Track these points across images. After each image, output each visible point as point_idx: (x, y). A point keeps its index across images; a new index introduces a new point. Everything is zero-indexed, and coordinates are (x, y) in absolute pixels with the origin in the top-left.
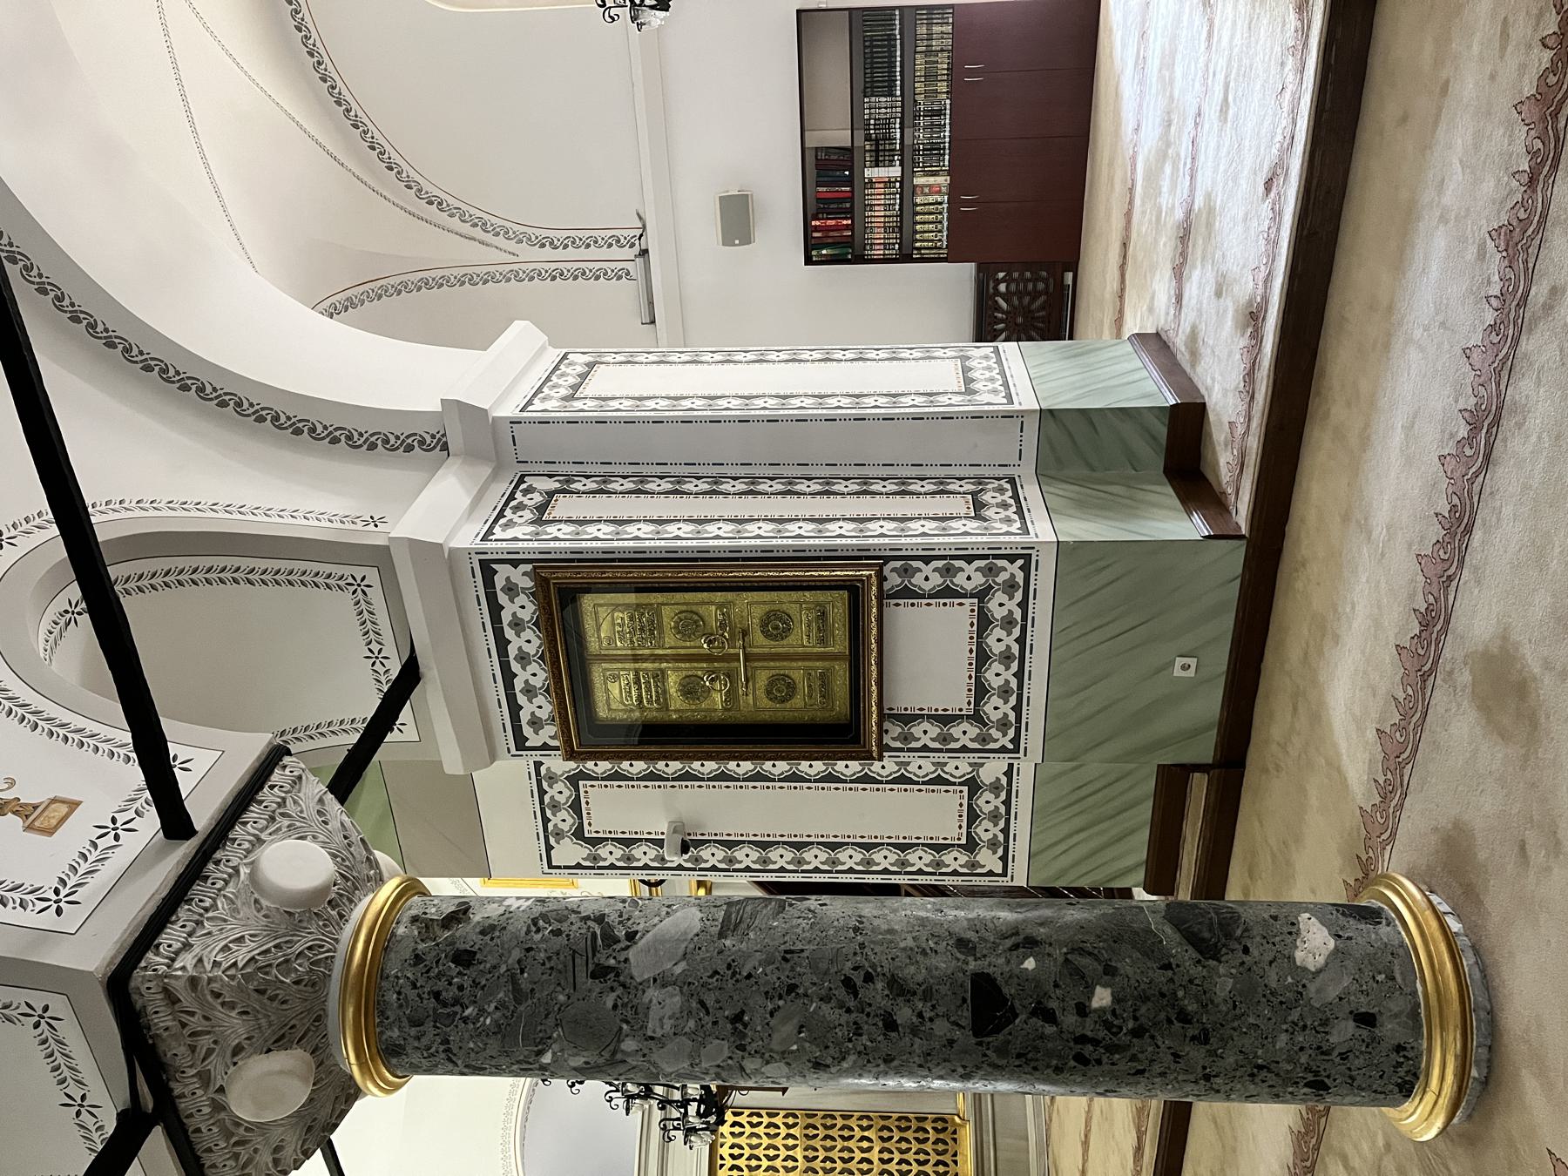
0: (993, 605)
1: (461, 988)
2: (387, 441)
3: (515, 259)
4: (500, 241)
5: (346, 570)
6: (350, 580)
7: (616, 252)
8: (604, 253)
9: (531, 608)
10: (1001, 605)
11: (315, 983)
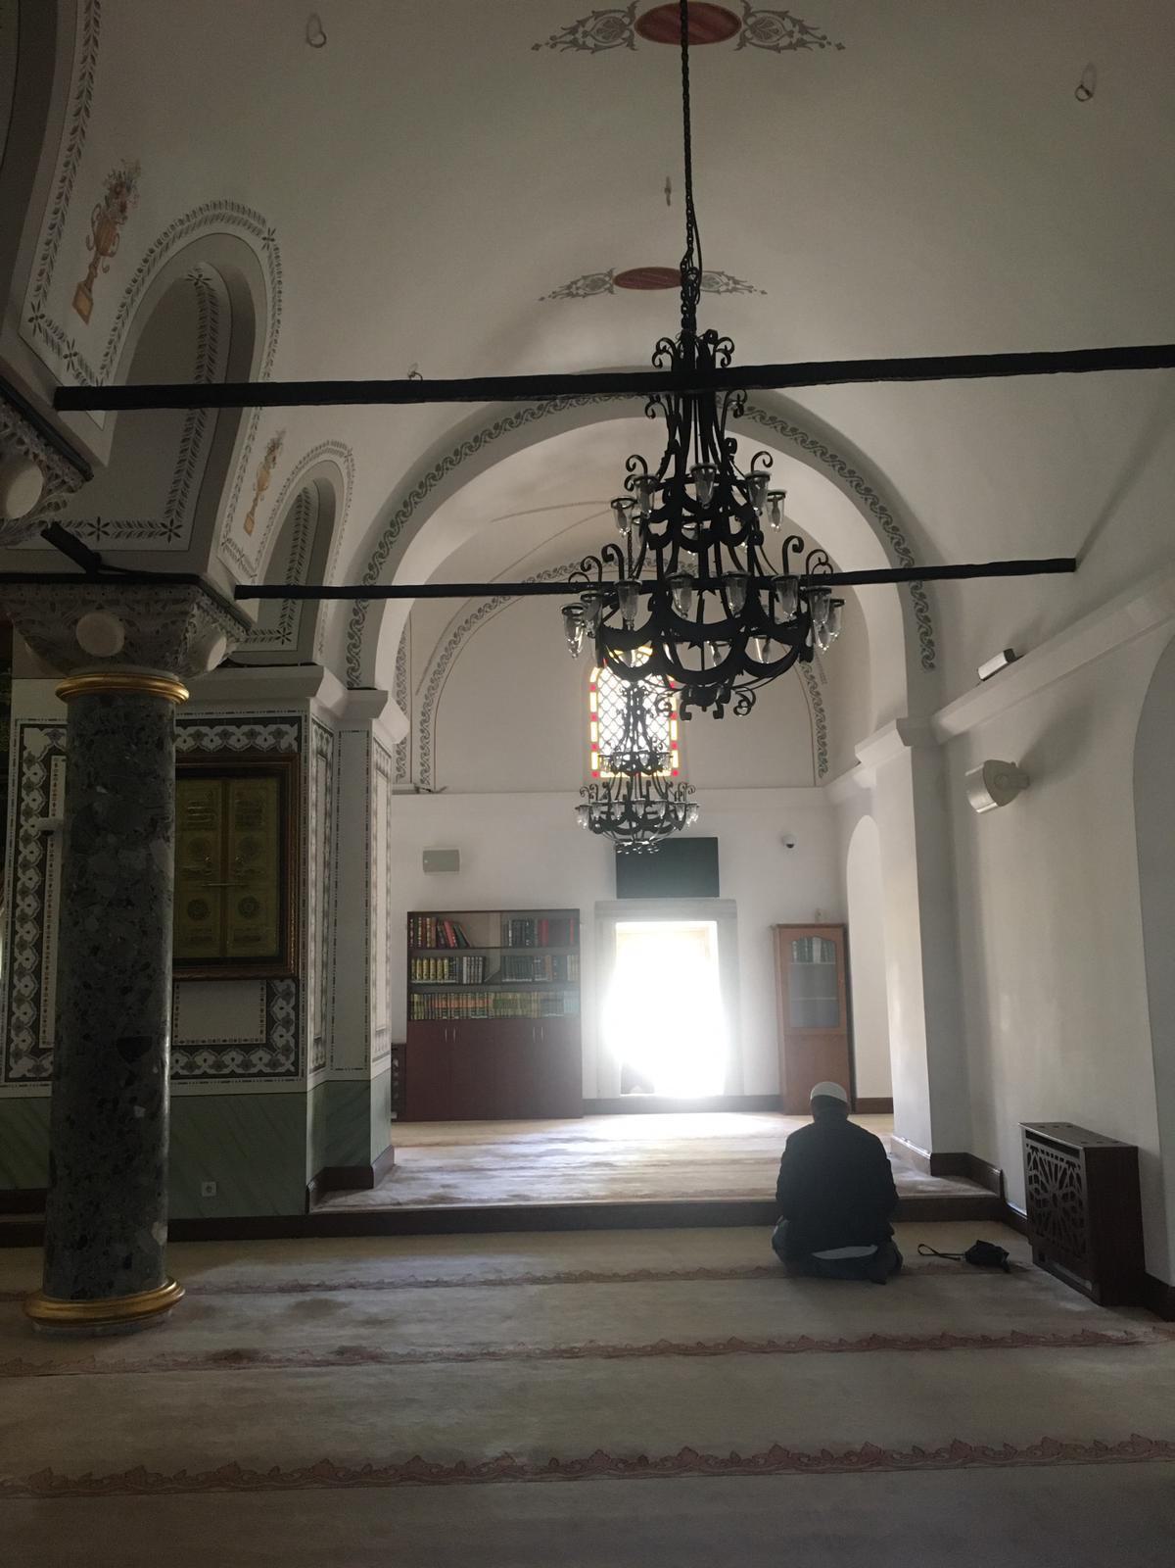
0: (261, 1053)
1: (147, 743)
2: (355, 646)
3: (414, 691)
4: (427, 683)
5: (295, 630)
6: (287, 631)
7: (417, 769)
8: (417, 760)
9: (265, 745)
10: (261, 1059)
11: (155, 664)
